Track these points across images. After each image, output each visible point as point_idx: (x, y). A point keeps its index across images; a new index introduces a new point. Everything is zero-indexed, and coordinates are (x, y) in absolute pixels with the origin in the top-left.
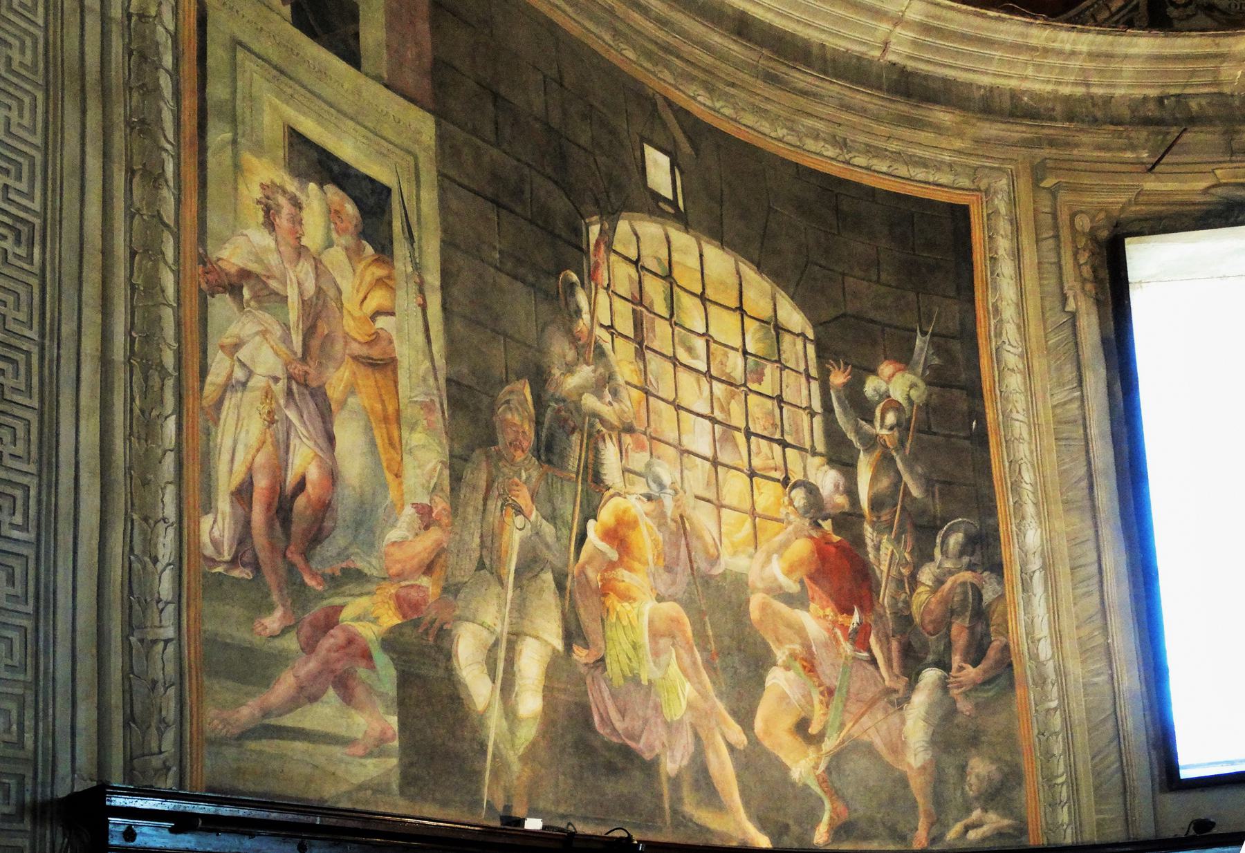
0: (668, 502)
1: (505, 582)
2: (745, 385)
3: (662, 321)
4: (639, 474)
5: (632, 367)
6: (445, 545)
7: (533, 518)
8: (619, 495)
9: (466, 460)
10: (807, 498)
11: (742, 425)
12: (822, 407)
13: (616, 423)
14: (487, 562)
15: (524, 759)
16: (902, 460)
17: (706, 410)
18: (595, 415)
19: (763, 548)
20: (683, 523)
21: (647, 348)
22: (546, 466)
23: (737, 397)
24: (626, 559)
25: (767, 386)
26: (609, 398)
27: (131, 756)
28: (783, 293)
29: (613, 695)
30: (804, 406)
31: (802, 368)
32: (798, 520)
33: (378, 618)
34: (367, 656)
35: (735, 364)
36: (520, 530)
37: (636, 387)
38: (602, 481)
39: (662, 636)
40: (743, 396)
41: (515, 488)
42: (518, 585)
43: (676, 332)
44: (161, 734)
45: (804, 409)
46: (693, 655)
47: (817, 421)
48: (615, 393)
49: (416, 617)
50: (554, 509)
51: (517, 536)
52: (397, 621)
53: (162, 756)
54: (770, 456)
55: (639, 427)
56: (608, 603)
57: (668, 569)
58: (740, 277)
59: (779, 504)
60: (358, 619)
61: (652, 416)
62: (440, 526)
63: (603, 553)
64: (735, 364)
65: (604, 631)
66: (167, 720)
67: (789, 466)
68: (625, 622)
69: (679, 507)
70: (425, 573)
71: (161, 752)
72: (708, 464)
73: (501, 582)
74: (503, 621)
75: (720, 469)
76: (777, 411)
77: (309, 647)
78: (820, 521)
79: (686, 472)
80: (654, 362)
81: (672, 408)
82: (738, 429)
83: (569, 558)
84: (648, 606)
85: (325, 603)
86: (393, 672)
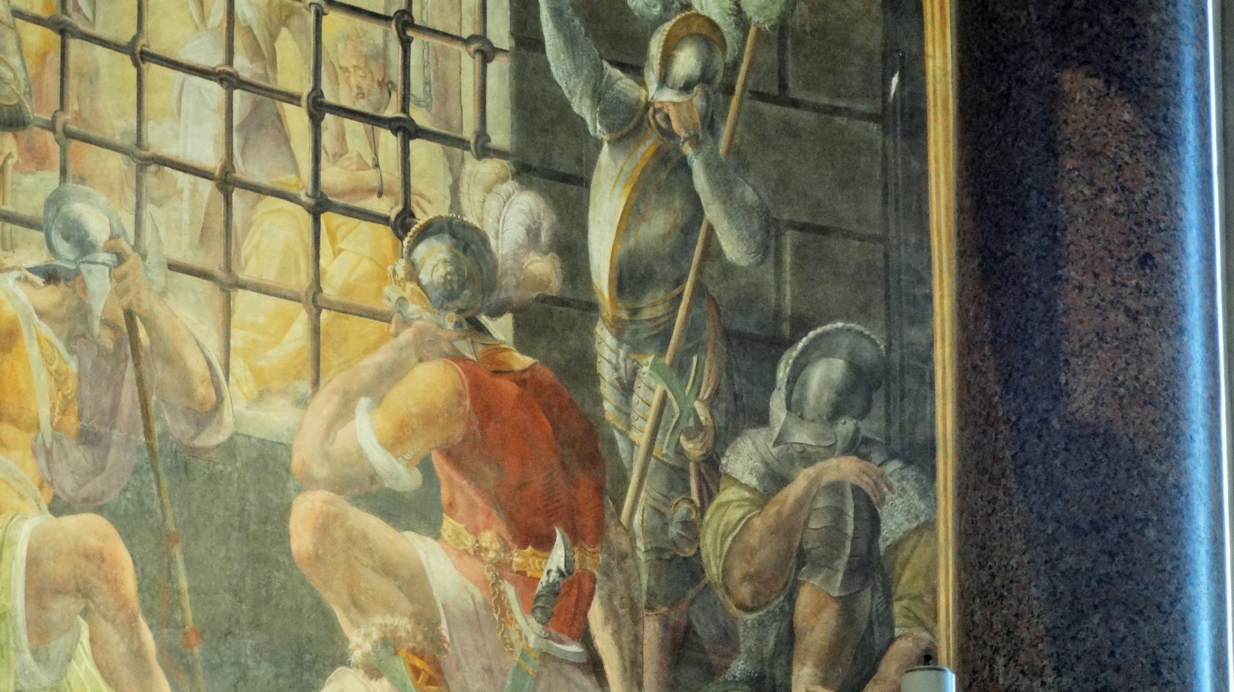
0: (99, 283)
4: (30, 224)
10: (455, 261)
11: (304, 88)
12: (513, 34)
16: (707, 165)
17: (213, 58)
19: (334, 382)
23: (295, 22)
32: (427, 315)
37: (37, 20)
39: (58, 592)
40: (311, 18)
45: (466, 42)
47: (499, 70)
54: (370, 163)
55: (36, 112)
57: (88, 438)
59: (383, 277)
61: (73, 83)
67: (415, 184)
69: (120, 293)
72: (206, 187)
75: (237, 197)
78: (484, 319)
79: (149, 209)
81: (126, 59)
82: (293, 99)
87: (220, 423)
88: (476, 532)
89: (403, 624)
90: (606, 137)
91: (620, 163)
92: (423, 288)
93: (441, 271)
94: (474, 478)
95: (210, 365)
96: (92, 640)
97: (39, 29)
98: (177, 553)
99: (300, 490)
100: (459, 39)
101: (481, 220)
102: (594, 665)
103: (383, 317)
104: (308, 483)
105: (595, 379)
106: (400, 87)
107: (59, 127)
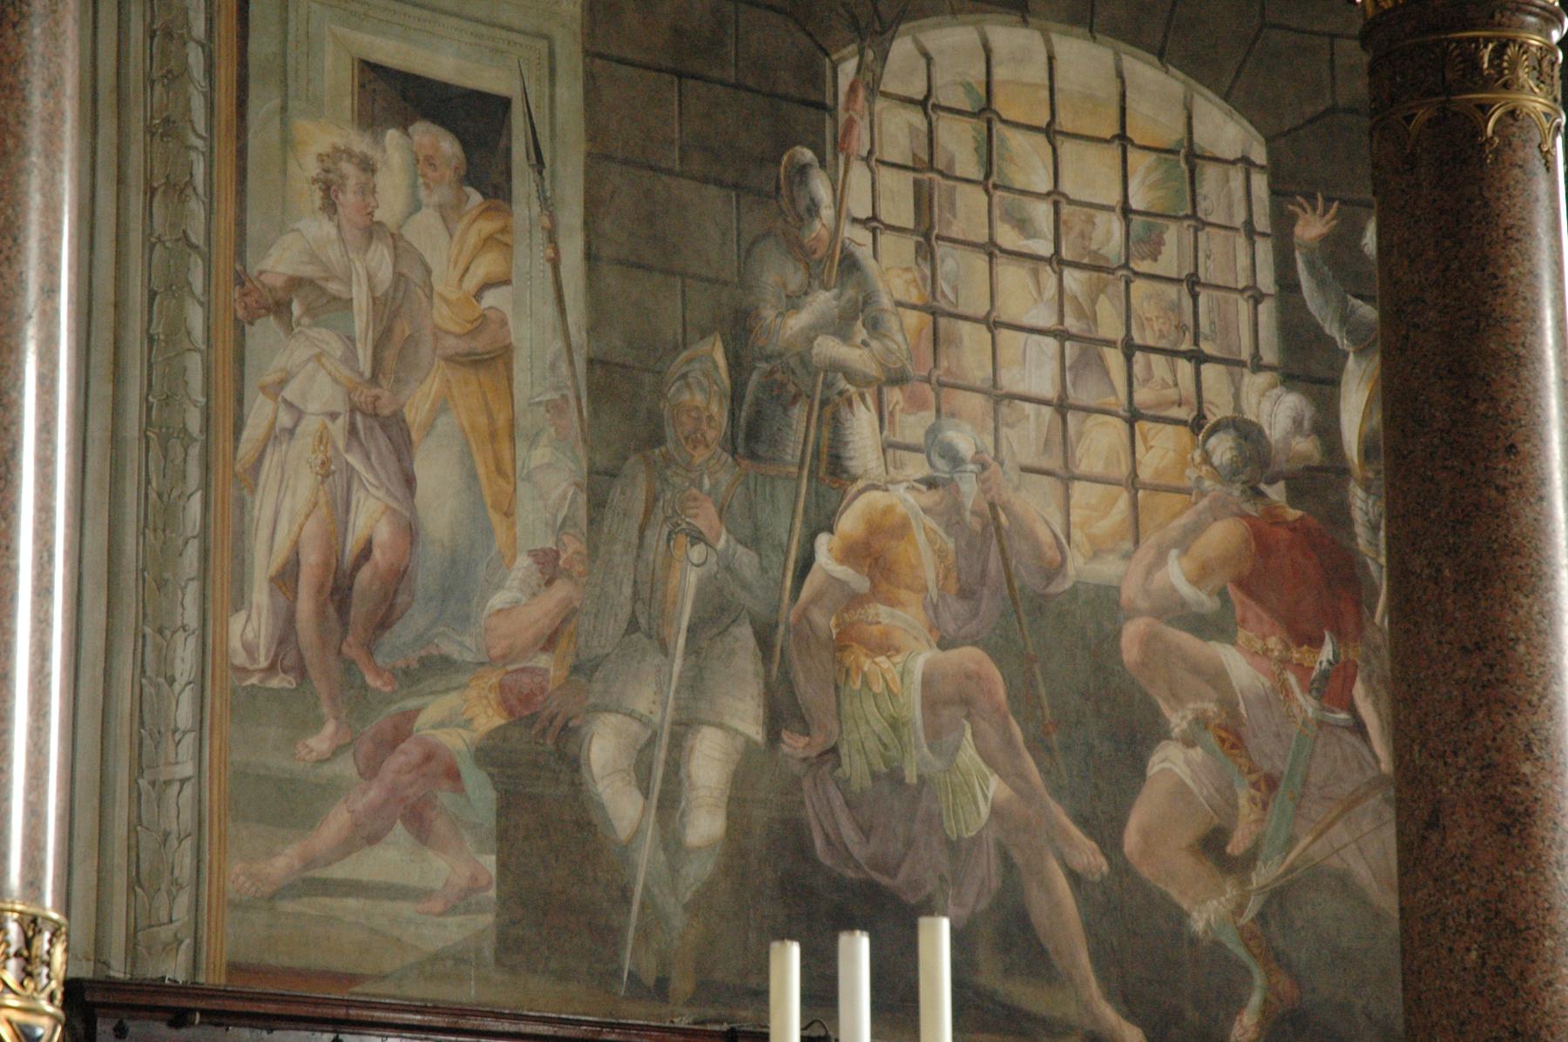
0: (969, 488)
1: (671, 651)
2: (1126, 266)
3: (967, 187)
5: (909, 276)
6: (577, 604)
7: (721, 544)
8: (875, 487)
9: (612, 474)
10: (1239, 447)
11: (1118, 334)
13: (873, 370)
14: (642, 621)
15: (691, 908)
17: (1046, 319)
18: (836, 367)
19: (1150, 541)
20: (996, 517)
21: (938, 237)
22: (745, 463)
23: (1110, 289)
24: (884, 587)
25: (1170, 261)
26: (861, 333)
27: (135, 927)
28: (1209, 94)
29: (847, 803)
30: (1241, 285)
31: (1239, 219)
32: (1218, 487)
33: (471, 720)
34: (453, 775)
35: (1109, 235)
36: (698, 566)
37: (914, 307)
38: (845, 471)
40: (1122, 285)
41: (692, 504)
42: (692, 648)
43: (996, 199)
44: (172, 899)
45: (1242, 291)
46: (1006, 729)
47: (1267, 311)
48: (874, 326)
49: (527, 713)
50: (756, 528)
51: (693, 577)
52: (499, 721)
53: (173, 926)
54: (1171, 383)
56: (849, 660)
57: (965, 593)
58: (1123, 82)
59: (1183, 463)
60: (441, 725)
62: (570, 577)
63: (842, 583)
64: (1109, 233)
65: (839, 704)
66: (180, 881)
67: (1206, 395)
68: (878, 687)
70: (544, 649)
71: (171, 921)
72: (1047, 412)
73: (664, 648)
74: (664, 706)
75: (1069, 417)
76: (1187, 302)
77: (370, 771)
78: (1263, 487)
79: (1004, 431)
80: (950, 260)
81: (984, 328)
82: (1110, 343)
83: (780, 599)
84: (922, 657)
85: (394, 708)
86: (492, 795)
87: (1065, 576)
88: (1264, 638)
89: (1211, 707)
90: (1351, 349)
91: (1363, 366)
92: (1215, 468)
93: (1228, 456)
94: (1260, 600)
95: (1055, 536)
96: (974, 735)
97: (915, 313)
98: (1037, 668)
99: (1128, 618)
100: (1236, 290)
101: (1258, 417)
102: (1359, 727)
103: (1186, 491)
104: (1133, 613)
105: (1348, 522)
106: (1192, 329)
107: (934, 380)
